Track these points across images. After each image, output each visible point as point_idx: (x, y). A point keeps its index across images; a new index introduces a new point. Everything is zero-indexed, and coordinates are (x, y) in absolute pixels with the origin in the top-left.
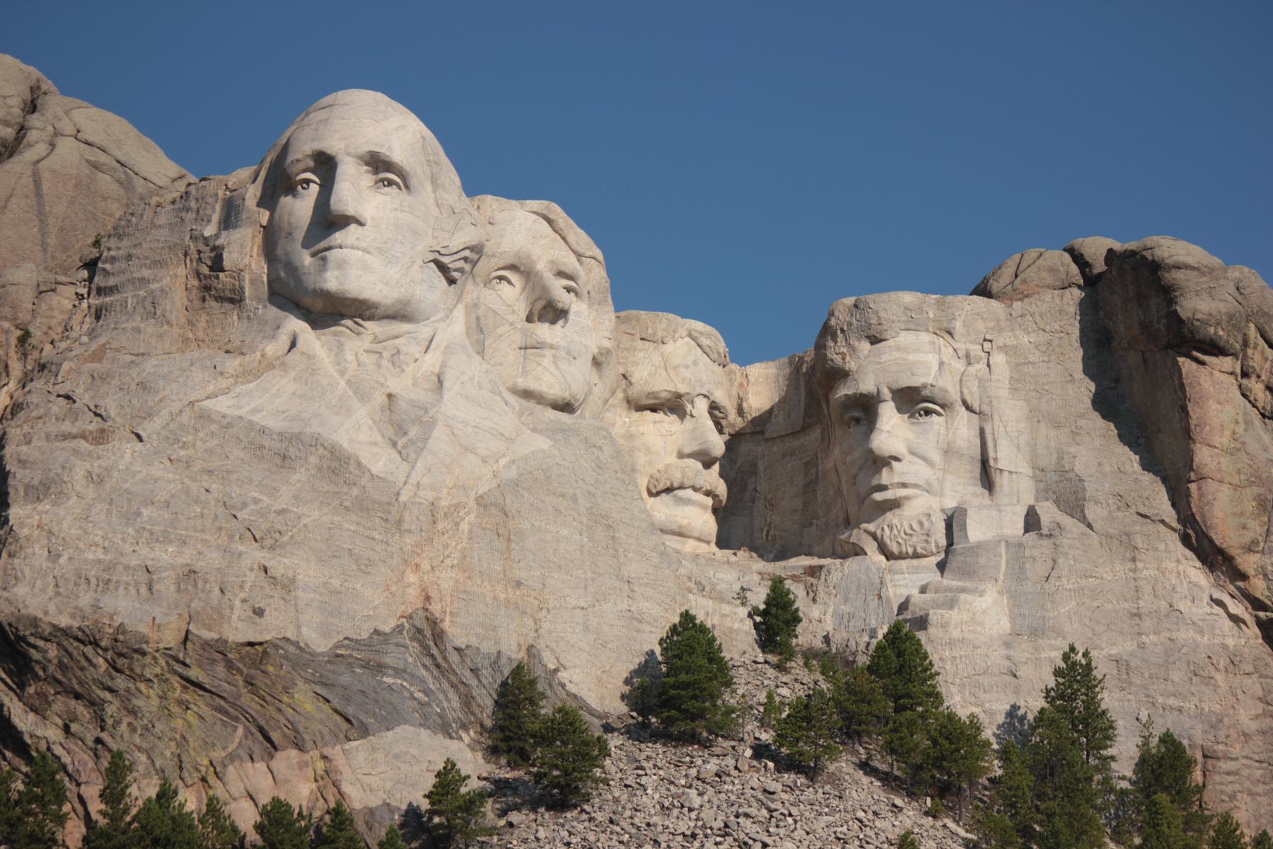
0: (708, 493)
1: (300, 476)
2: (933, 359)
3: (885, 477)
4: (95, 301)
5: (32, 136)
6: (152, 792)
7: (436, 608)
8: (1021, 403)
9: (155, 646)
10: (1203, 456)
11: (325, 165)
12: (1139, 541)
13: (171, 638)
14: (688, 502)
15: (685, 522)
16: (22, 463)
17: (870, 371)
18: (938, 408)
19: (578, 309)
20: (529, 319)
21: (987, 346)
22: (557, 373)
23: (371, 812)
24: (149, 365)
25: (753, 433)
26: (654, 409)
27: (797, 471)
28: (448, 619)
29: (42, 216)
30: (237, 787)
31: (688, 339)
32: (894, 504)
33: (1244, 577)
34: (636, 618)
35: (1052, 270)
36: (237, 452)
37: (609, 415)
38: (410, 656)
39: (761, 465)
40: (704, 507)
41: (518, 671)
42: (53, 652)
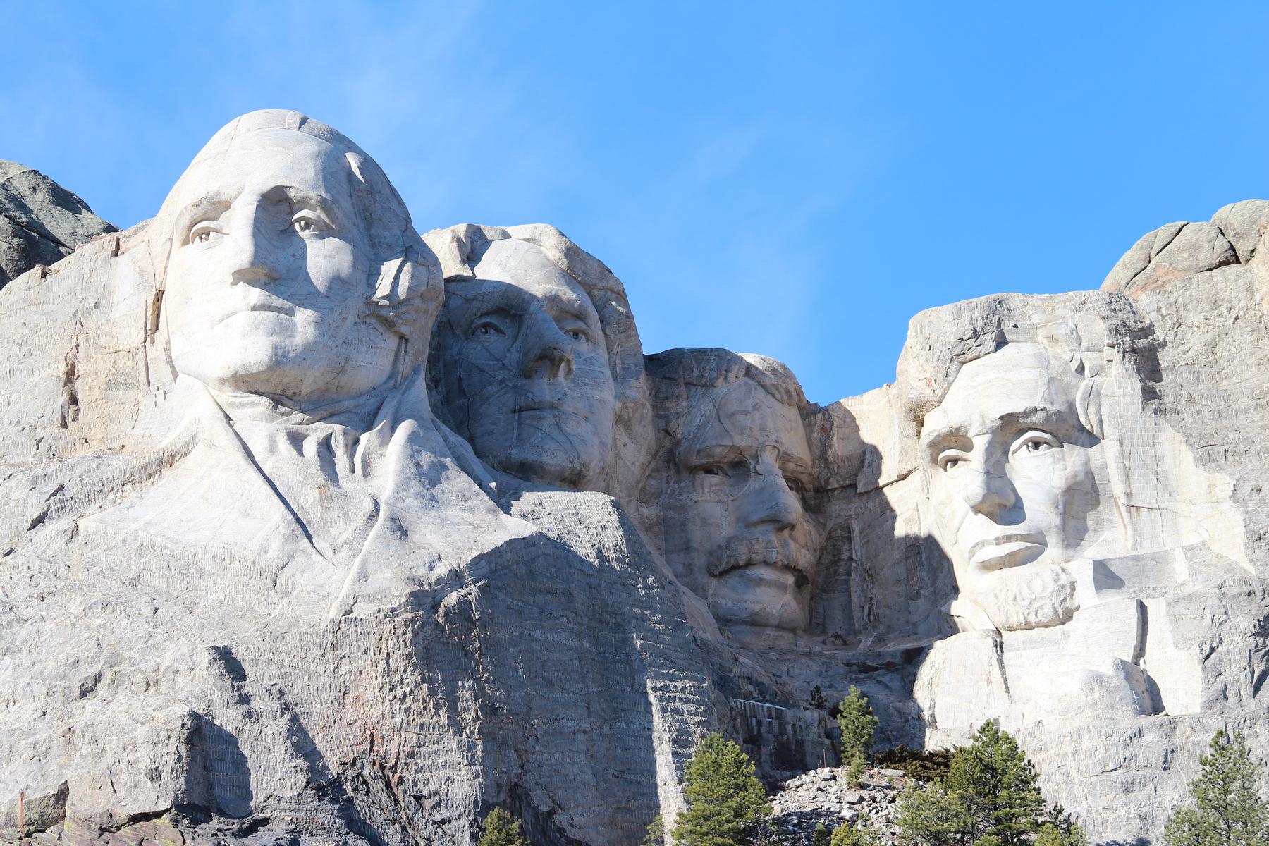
0: (788, 568)
8: (1160, 420)
9: (26, 830)
14: (760, 582)
15: (758, 607)
18: (1048, 437)
21: (1109, 353)
22: (561, 438)
25: (844, 488)
26: (709, 471)
28: (402, 761)
31: (747, 379)
35: (1195, 248)
37: (652, 482)
39: (856, 528)
40: (783, 587)
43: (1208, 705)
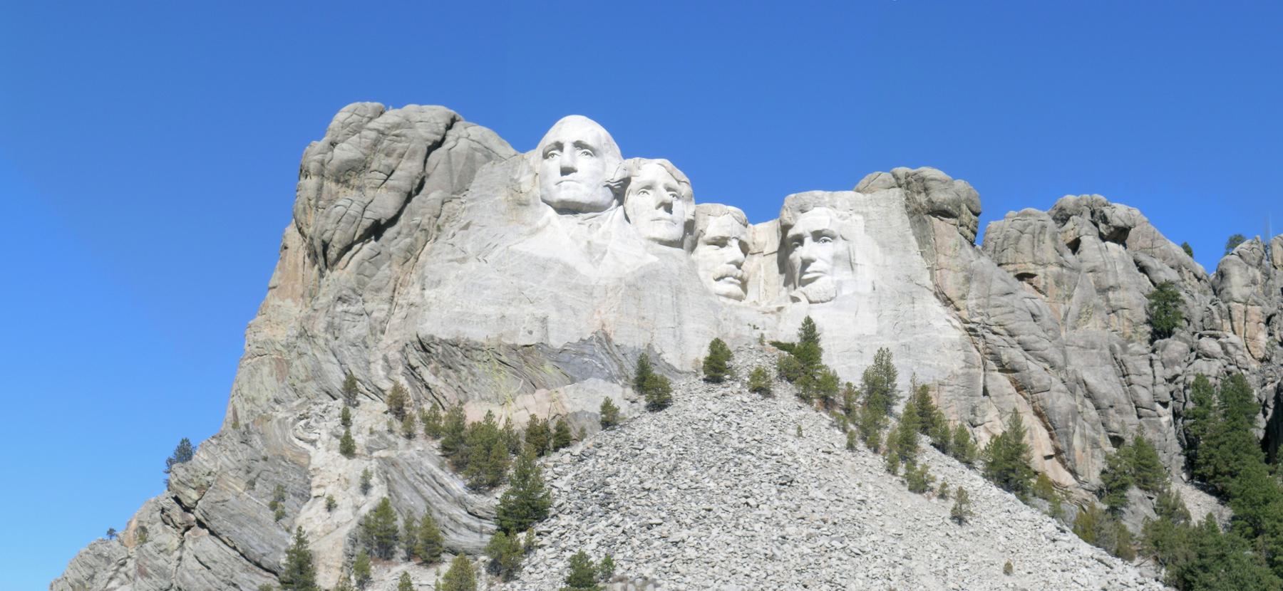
3: (808, 270)
5: (448, 138)
7: (607, 329)
10: (942, 259)
12: (915, 295)
17: (802, 225)
23: (576, 414)
24: (485, 230)
29: (451, 172)
33: (958, 310)
42: (440, 350)
43: (879, 333)
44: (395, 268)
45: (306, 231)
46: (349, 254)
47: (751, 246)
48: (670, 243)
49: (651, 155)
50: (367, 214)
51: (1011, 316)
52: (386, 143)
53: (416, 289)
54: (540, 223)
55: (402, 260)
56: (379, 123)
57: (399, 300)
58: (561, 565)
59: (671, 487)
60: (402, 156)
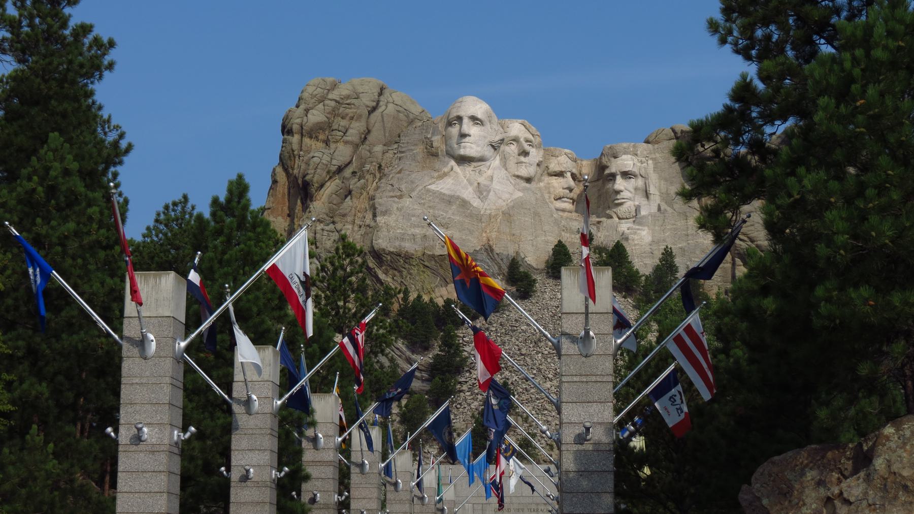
1: (454, 207)
2: (631, 163)
3: (618, 197)
4: (399, 155)
5: (381, 103)
6: (416, 296)
7: (491, 243)
11: (460, 119)
13: (420, 254)
16: (380, 205)
17: (615, 166)
19: (533, 151)
20: (519, 155)
24: (413, 176)
27: (596, 193)
30: (438, 294)
32: (621, 204)
34: (547, 242)
36: (437, 200)
38: (484, 256)
41: (513, 259)
42: (389, 258)
44: (355, 200)
45: (291, 171)
46: (323, 190)
47: (578, 176)
48: (528, 180)
49: (514, 116)
50: (334, 162)
51: (752, 228)
52: (341, 109)
53: (369, 216)
54: (446, 170)
55: (358, 196)
56: (334, 95)
57: (358, 222)
58: (476, 403)
59: (538, 353)
60: (352, 118)
